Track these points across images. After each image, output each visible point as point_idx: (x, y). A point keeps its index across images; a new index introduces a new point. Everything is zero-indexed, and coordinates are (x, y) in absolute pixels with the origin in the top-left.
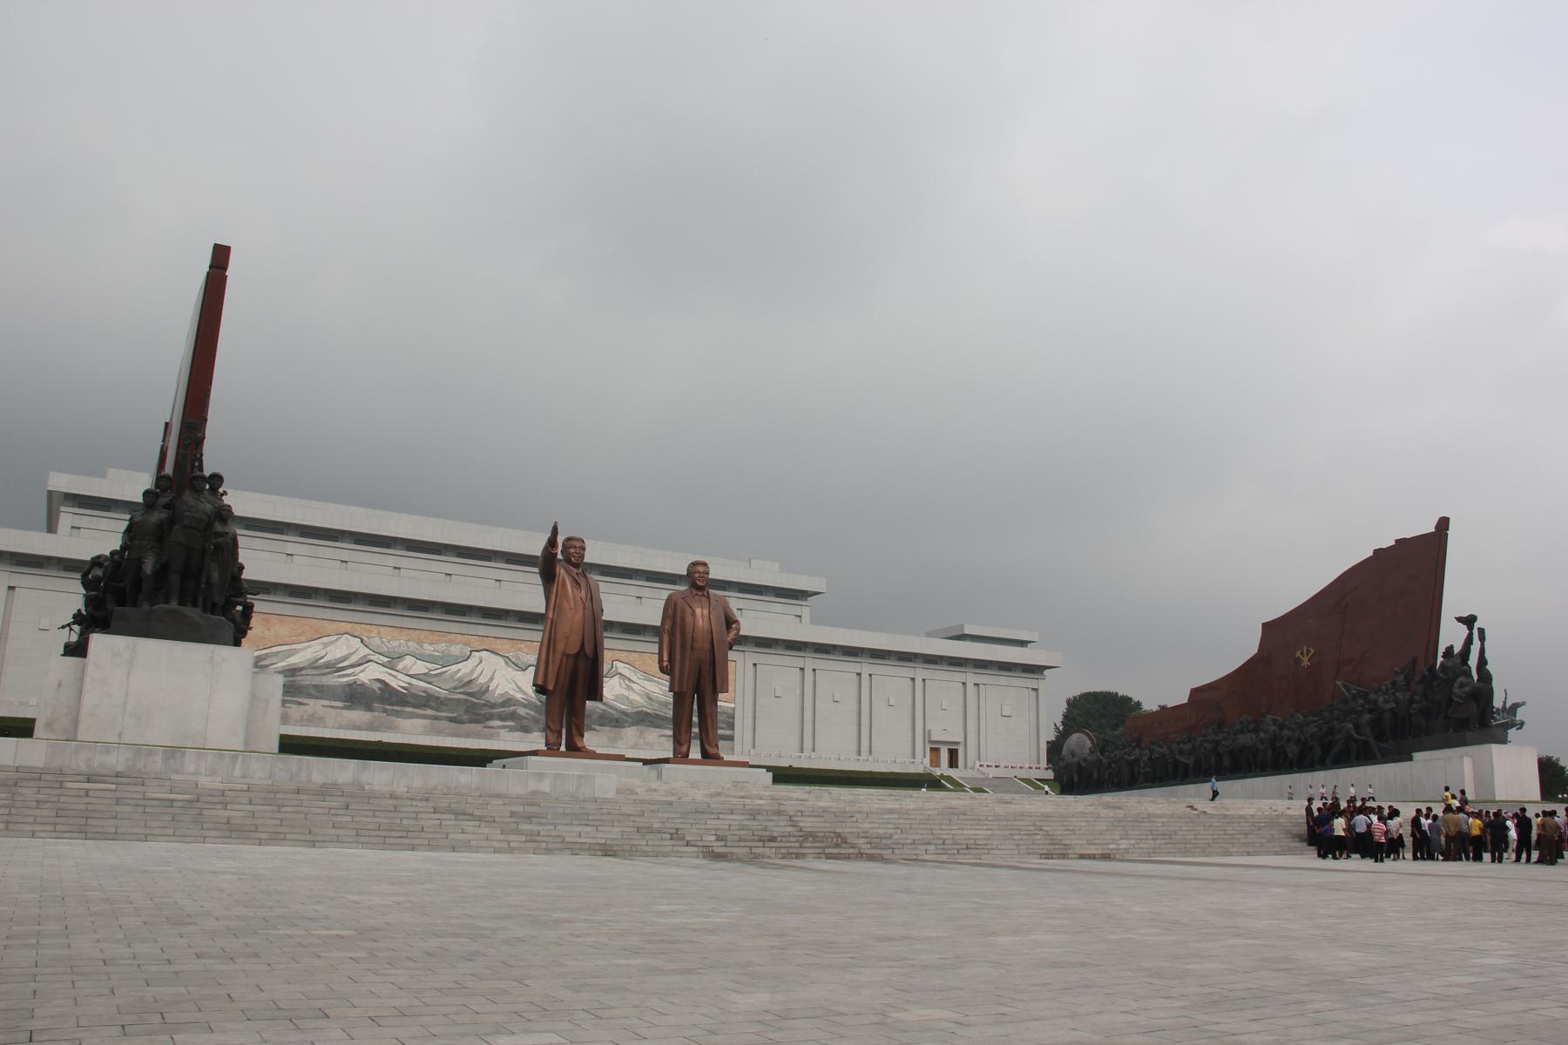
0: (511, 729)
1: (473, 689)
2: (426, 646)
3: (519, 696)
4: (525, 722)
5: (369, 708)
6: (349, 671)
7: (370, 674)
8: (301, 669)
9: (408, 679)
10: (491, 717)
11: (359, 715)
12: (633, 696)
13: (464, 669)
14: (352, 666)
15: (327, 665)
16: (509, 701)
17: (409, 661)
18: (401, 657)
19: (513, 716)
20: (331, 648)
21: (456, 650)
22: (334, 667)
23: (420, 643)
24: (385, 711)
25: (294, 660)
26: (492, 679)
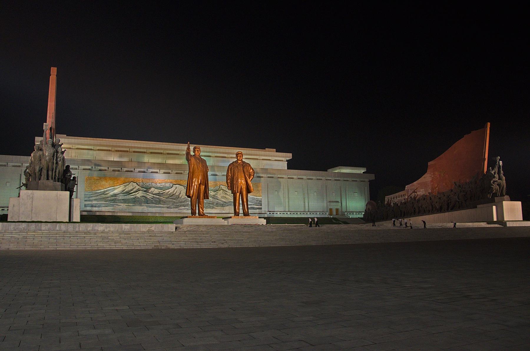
1: (174, 197)
7: (140, 194)
9: (153, 195)
10: (181, 206)
12: (227, 196)
13: (171, 190)
14: (134, 192)
15: (126, 193)
17: (152, 189)
18: (150, 188)
22: (128, 193)
25: (116, 192)
26: (180, 194)
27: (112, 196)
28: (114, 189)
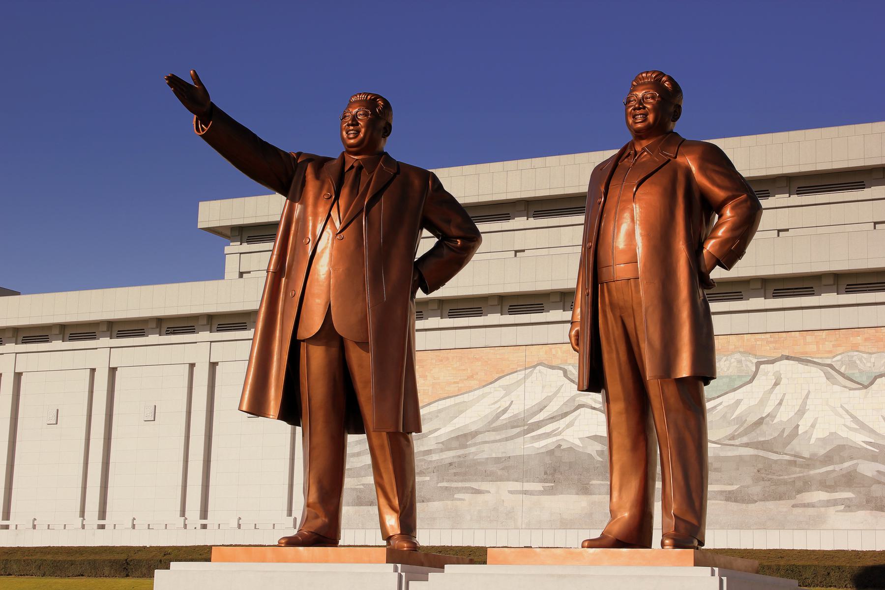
0: (849, 506)
3: (859, 439)
5: (585, 490)
8: (475, 434)
10: (806, 485)
14: (553, 419)
15: (514, 423)
16: (839, 451)
19: (850, 480)
26: (801, 412)
27: (446, 446)
28: (460, 410)
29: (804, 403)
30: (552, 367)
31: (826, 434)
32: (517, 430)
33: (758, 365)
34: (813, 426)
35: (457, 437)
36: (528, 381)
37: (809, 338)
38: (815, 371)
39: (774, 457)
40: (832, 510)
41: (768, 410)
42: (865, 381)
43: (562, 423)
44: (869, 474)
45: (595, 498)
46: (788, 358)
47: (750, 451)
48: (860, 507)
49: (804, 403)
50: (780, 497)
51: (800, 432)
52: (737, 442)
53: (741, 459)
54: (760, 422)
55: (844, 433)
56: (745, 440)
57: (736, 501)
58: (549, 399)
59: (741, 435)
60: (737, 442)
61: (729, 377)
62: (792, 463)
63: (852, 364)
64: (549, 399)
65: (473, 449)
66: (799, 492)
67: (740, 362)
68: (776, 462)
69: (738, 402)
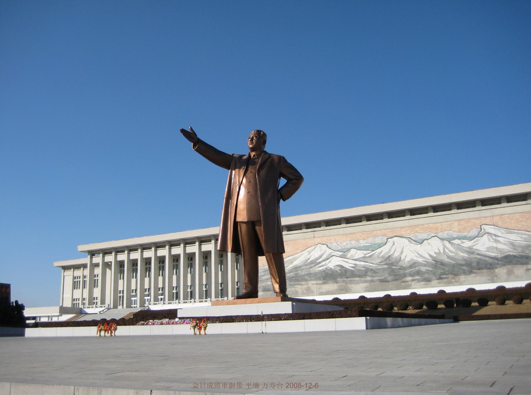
0: (419, 281)
2: (361, 241)
3: (420, 260)
4: (426, 276)
6: (323, 263)
7: (333, 263)
8: (300, 267)
9: (354, 262)
10: (405, 276)
11: (331, 286)
12: (500, 246)
13: (384, 250)
14: (324, 260)
15: (312, 262)
16: (414, 264)
17: (353, 251)
18: (349, 250)
19: (418, 273)
20: (313, 253)
21: (378, 240)
23: (358, 240)
24: (344, 281)
26: (402, 253)
28: (295, 259)
29: (402, 250)
30: (323, 244)
31: (410, 259)
32: (313, 265)
33: (387, 239)
34: (406, 257)
35: (295, 268)
36: (316, 250)
37: (403, 230)
38: (404, 239)
39: (395, 267)
40: (413, 283)
41: (391, 253)
42: (421, 242)
43: (327, 261)
44: (424, 270)
45: (339, 284)
46: (396, 236)
47: (386, 266)
48: (422, 281)
49: (402, 250)
50: (396, 280)
51: (402, 259)
52: (383, 264)
53: (384, 269)
54: (390, 256)
55: (415, 258)
56: (385, 263)
57: (383, 282)
58: (322, 255)
59: (383, 261)
60: (383, 264)
61: (379, 244)
62: (400, 269)
63: (416, 237)
64: (322, 255)
65: (300, 272)
66: (403, 278)
67: (381, 239)
68: (395, 269)
69: (382, 251)
